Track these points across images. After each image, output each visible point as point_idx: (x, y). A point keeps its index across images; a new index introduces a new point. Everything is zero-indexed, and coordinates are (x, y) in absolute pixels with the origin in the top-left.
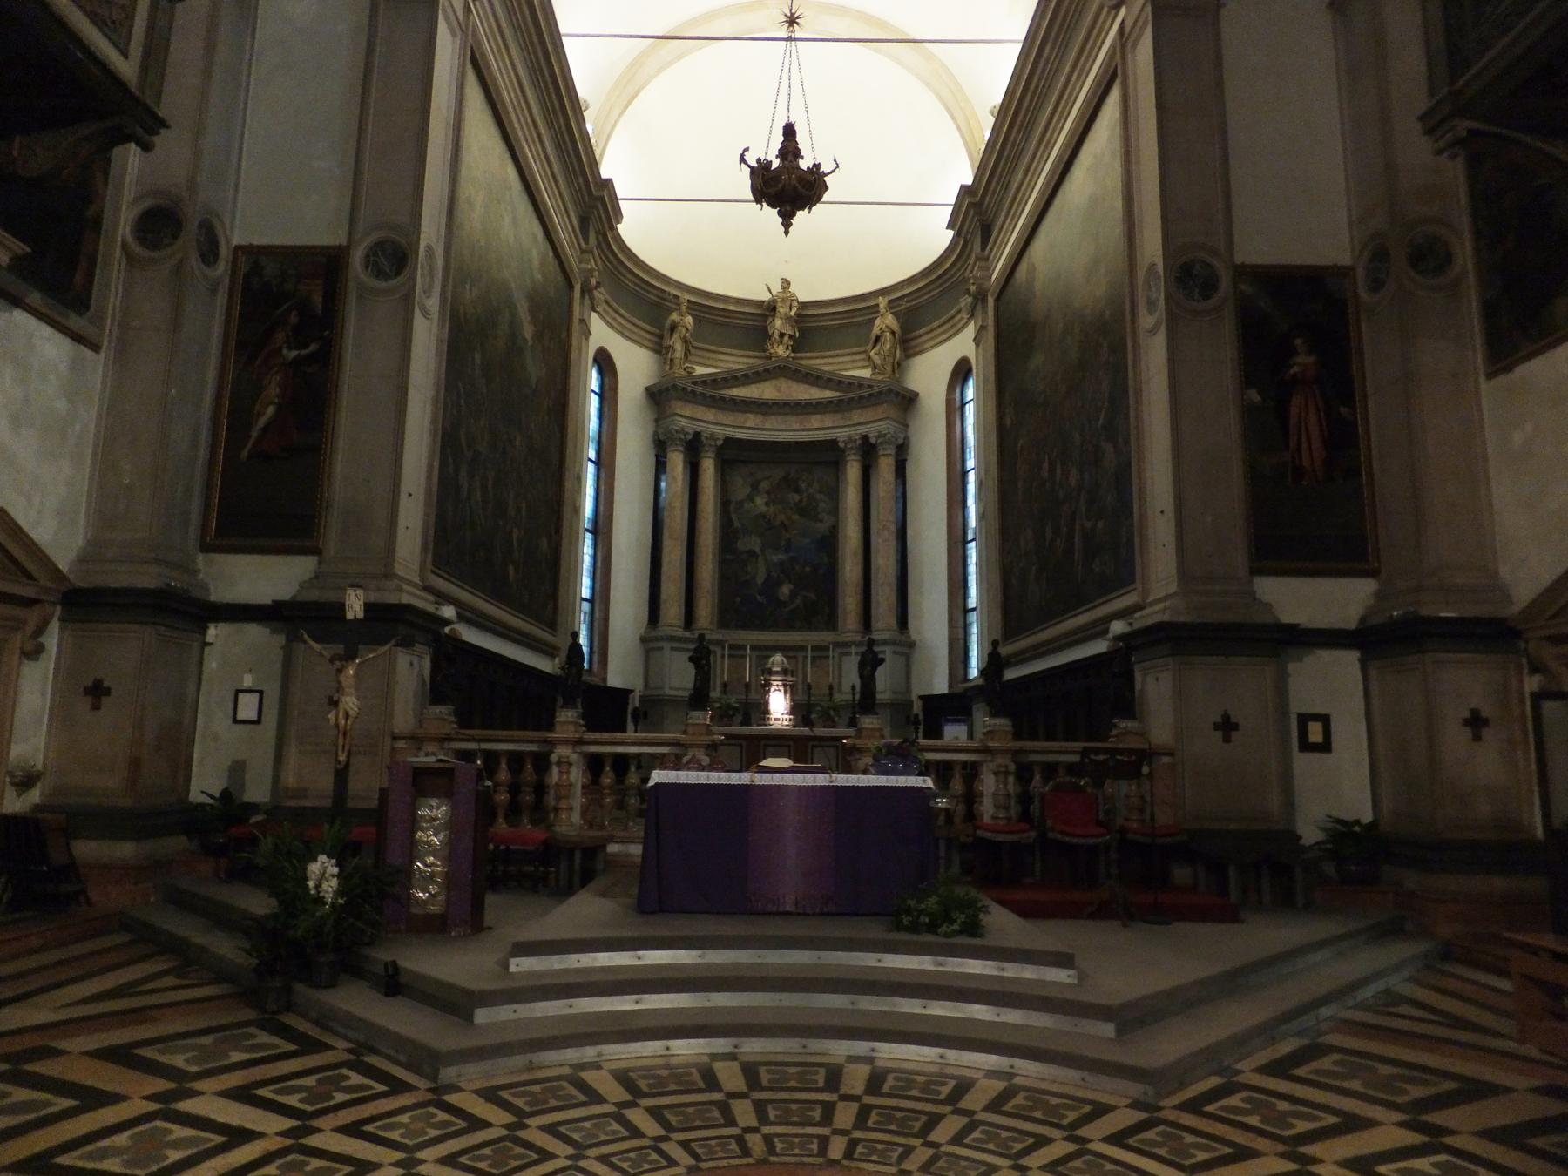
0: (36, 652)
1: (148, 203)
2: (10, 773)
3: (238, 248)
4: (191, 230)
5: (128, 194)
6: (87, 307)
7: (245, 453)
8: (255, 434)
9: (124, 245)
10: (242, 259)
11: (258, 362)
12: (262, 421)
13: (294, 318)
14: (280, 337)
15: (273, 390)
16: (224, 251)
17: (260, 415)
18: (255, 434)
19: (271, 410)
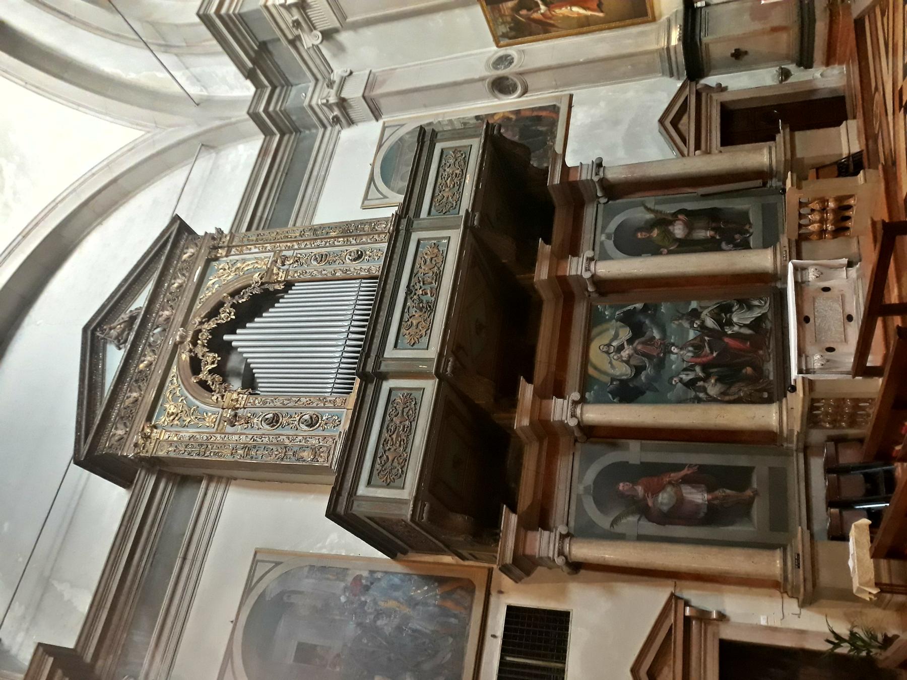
0: (719, 85)
1: (496, 92)
2: (782, 81)
3: (498, 46)
4: (502, 72)
5: (496, 102)
6: (555, 106)
7: (601, 15)
8: (589, 13)
9: (520, 96)
10: (502, 43)
11: (552, 22)
12: (582, 11)
13: (524, 12)
14: (536, 15)
15: (564, 11)
16: (502, 52)
17: (578, 13)
18: (589, 13)
19: (575, 9)
